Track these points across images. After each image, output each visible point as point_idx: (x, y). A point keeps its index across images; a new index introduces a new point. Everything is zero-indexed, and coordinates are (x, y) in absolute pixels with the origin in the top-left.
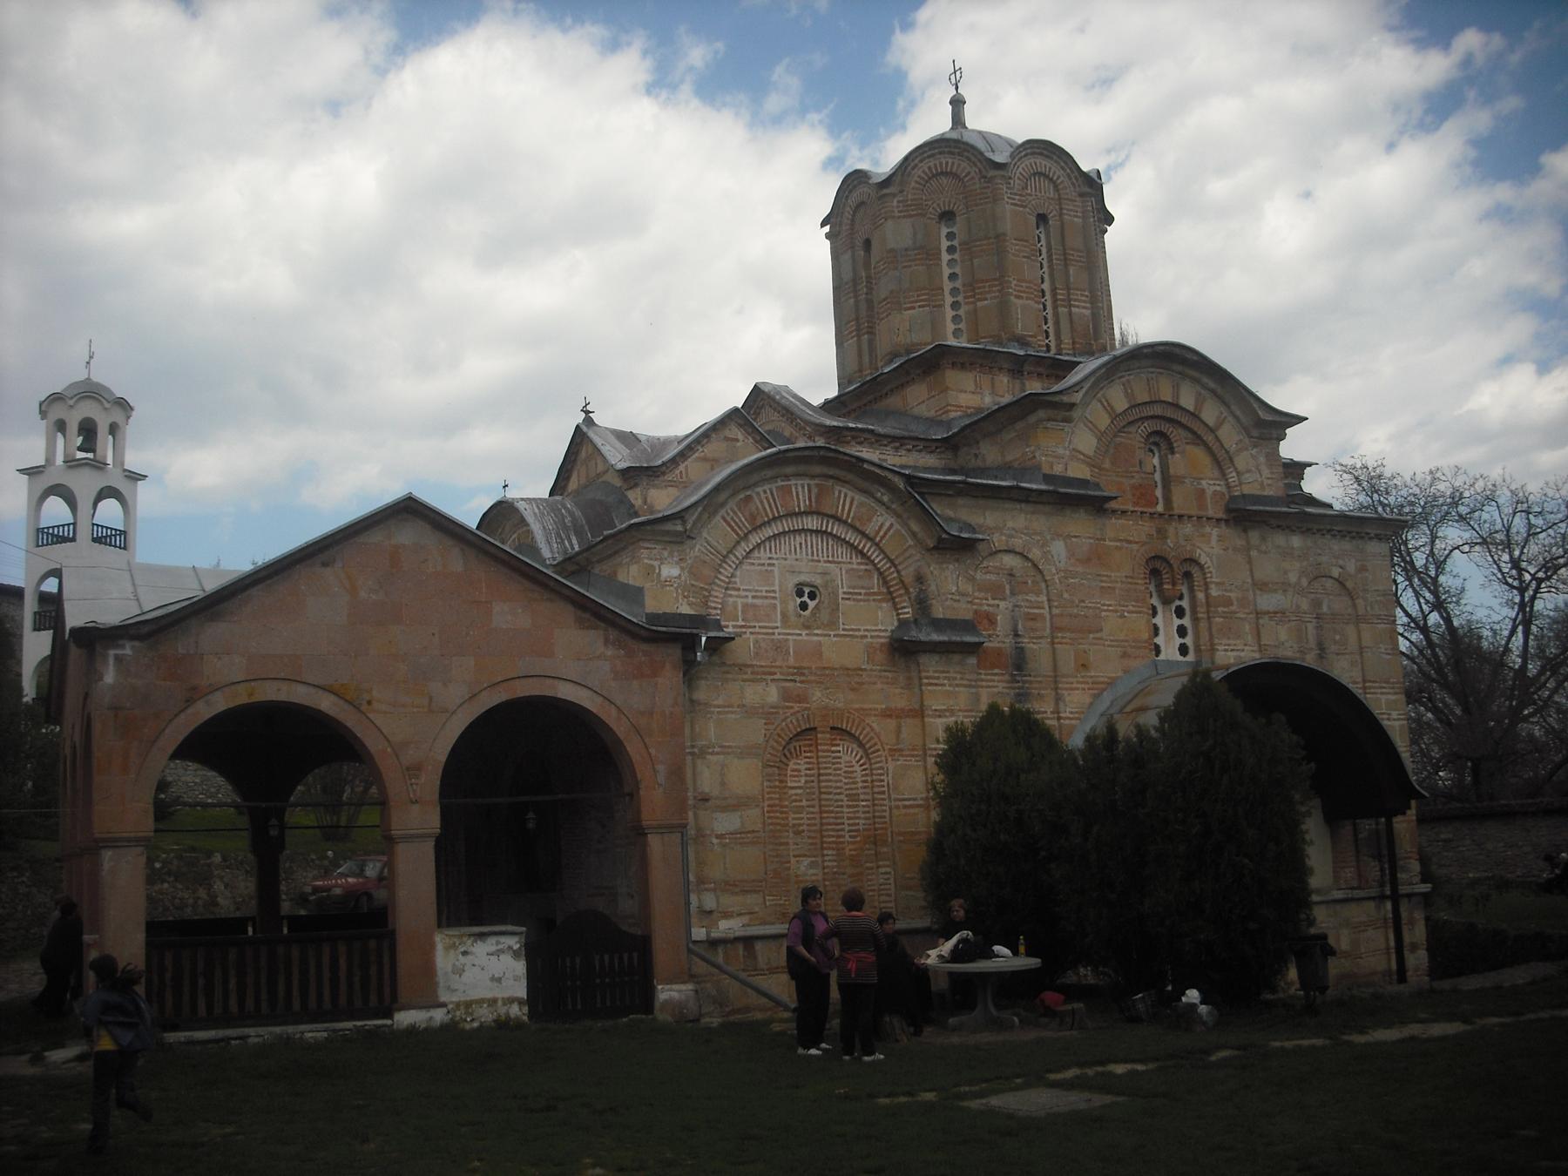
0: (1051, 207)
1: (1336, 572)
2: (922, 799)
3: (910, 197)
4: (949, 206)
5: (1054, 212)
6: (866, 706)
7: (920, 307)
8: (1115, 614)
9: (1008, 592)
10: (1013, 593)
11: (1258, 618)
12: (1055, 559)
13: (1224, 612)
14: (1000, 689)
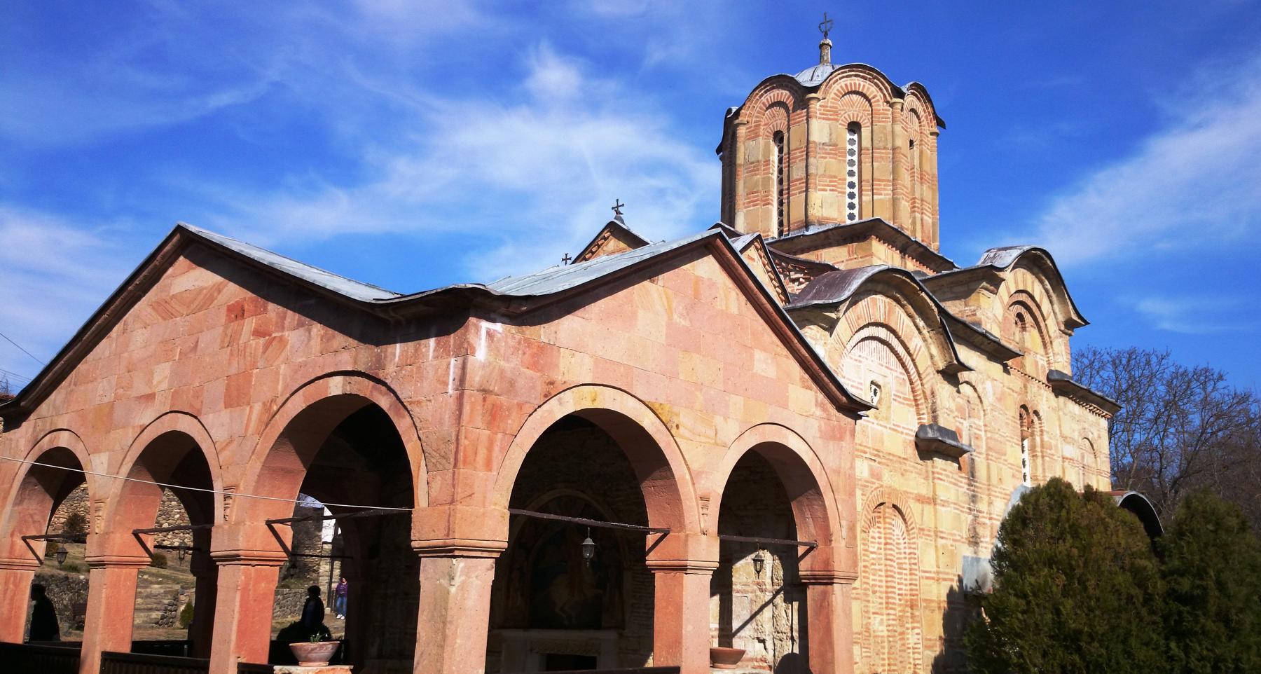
2: (934, 573)
3: (829, 104)
4: (857, 118)
6: (909, 490)
7: (831, 190)
11: (1063, 462)
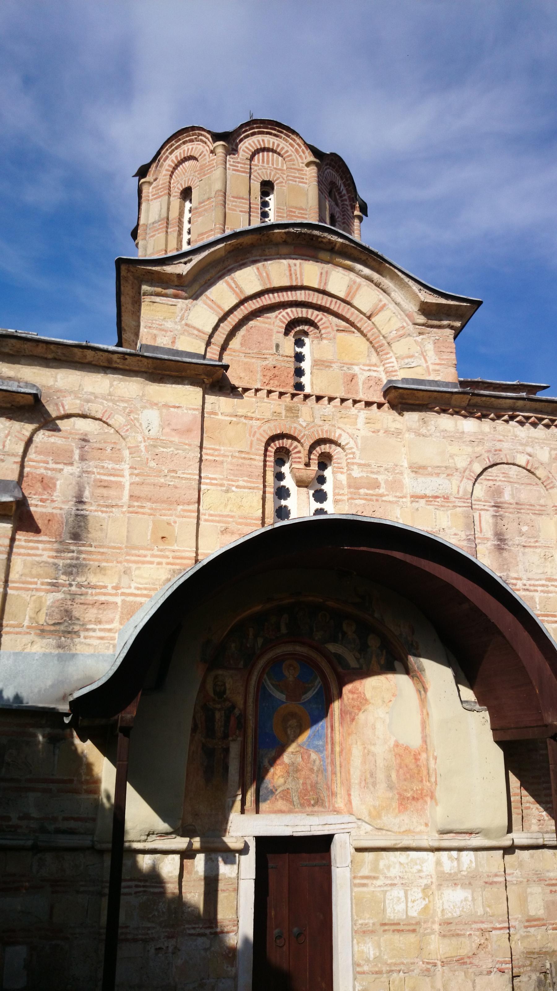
0: (278, 176)
1: (522, 460)
3: (161, 182)
5: (281, 179)
8: (219, 488)
9: (76, 457)
10: (83, 458)
12: (144, 427)
13: (367, 495)
14: (45, 558)
